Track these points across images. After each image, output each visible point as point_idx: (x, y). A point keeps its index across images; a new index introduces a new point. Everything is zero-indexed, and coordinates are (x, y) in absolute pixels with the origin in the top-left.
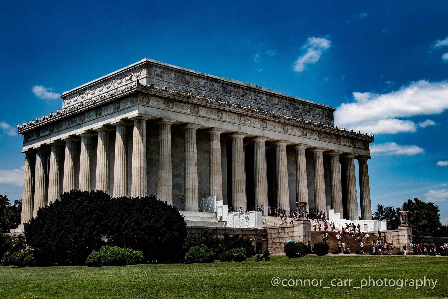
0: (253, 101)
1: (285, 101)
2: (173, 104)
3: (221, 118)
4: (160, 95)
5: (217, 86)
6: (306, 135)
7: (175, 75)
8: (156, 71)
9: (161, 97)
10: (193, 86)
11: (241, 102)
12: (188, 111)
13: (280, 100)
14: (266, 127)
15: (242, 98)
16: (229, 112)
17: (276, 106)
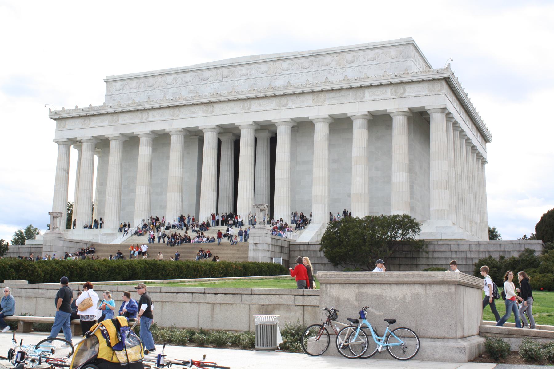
0: (245, 77)
1: (303, 60)
2: (90, 120)
3: (146, 119)
4: (71, 115)
5: (190, 77)
6: (287, 105)
7: (137, 83)
8: (115, 86)
9: (73, 117)
10: (159, 87)
11: (224, 85)
12: (107, 123)
13: (291, 62)
14: (213, 112)
15: (226, 79)
16: (153, 109)
17: (284, 73)
